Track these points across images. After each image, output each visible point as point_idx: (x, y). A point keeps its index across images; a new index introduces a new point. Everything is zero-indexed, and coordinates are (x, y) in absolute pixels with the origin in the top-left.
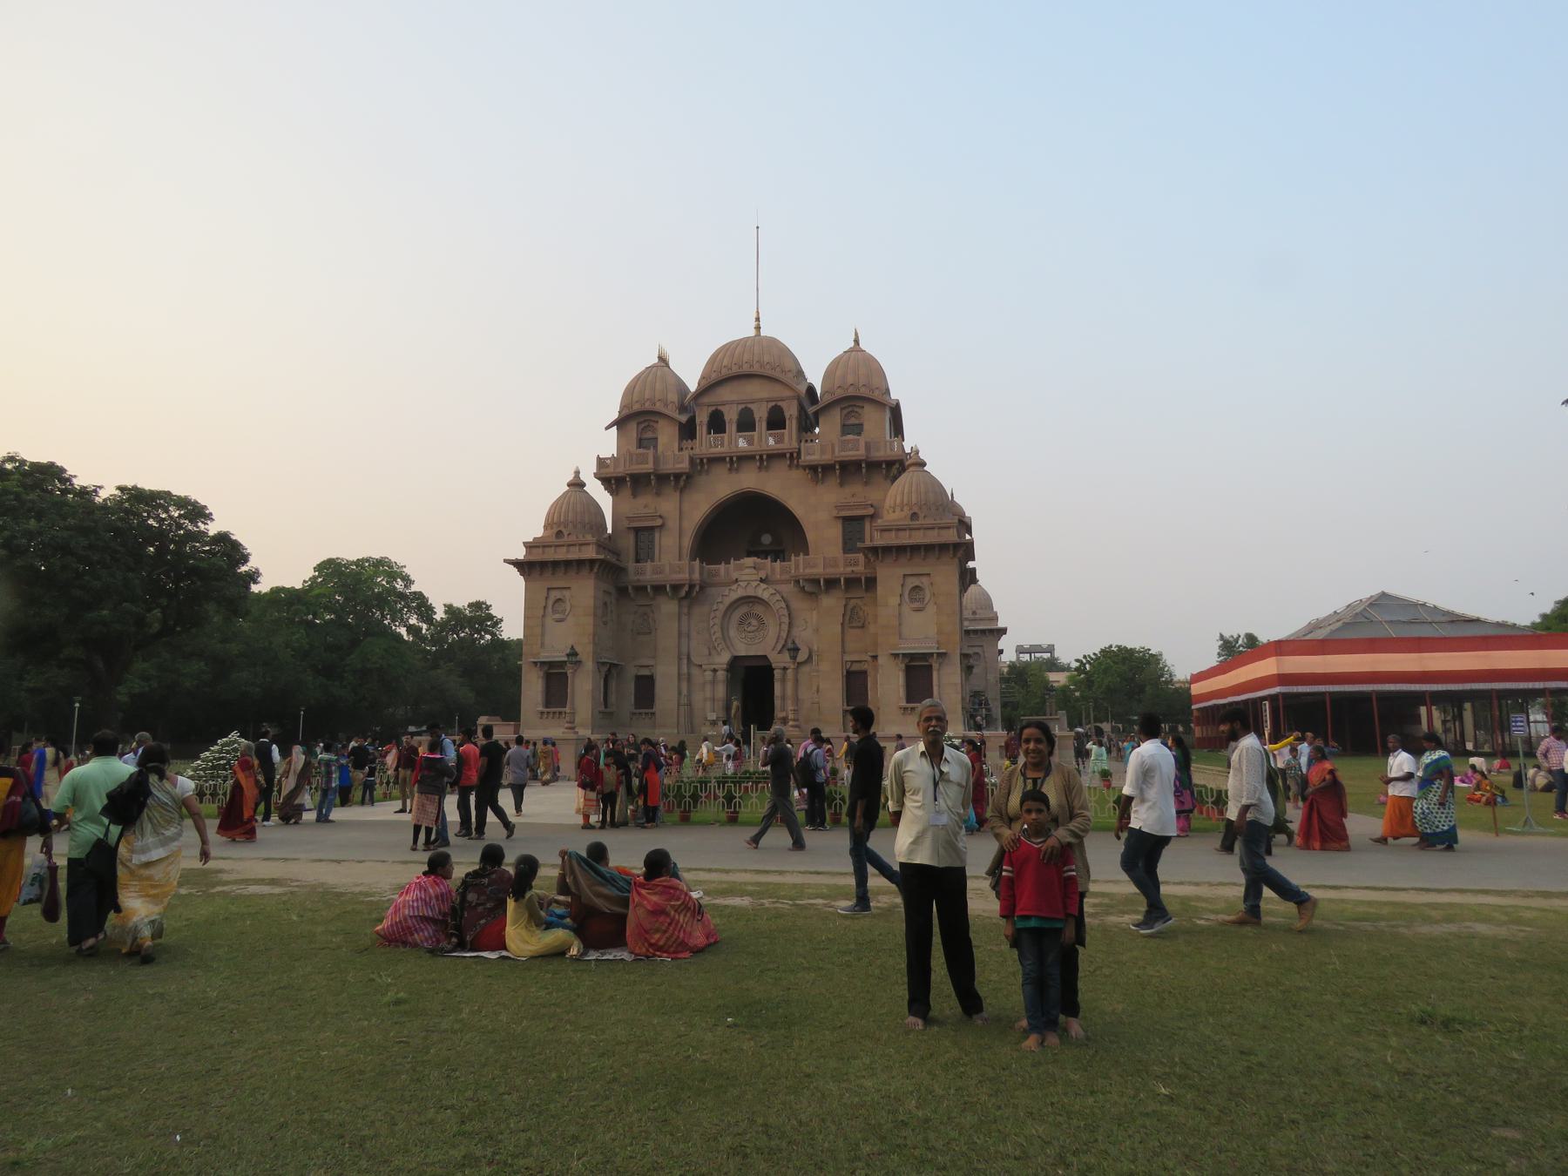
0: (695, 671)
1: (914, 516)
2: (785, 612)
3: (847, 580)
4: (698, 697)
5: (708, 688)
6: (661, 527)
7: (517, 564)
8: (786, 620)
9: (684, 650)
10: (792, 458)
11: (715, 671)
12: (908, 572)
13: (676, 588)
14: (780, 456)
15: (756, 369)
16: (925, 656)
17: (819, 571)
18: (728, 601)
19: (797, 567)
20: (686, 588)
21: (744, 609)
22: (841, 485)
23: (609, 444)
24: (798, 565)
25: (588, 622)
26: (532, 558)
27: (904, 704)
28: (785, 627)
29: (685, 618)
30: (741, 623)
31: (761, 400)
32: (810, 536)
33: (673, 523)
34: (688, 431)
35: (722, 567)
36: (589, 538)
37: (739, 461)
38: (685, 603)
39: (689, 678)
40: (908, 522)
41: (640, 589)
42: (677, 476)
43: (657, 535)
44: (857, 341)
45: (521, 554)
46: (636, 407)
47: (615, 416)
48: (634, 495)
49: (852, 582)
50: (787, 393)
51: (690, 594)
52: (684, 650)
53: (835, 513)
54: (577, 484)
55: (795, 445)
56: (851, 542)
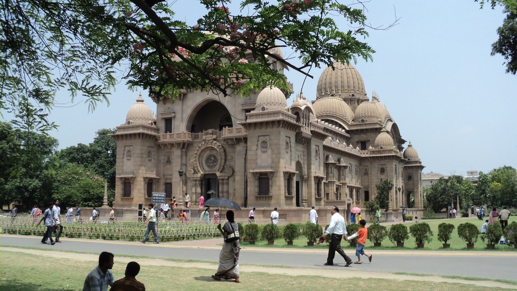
2: (223, 154)
6: (174, 117)
8: (223, 157)
13: (179, 144)
16: (266, 174)
20: (182, 145)
24: (226, 133)
28: (223, 161)
29: (184, 157)
30: (208, 159)
33: (178, 116)
35: (200, 134)
38: (184, 150)
40: (261, 111)
41: (165, 145)
48: (164, 103)
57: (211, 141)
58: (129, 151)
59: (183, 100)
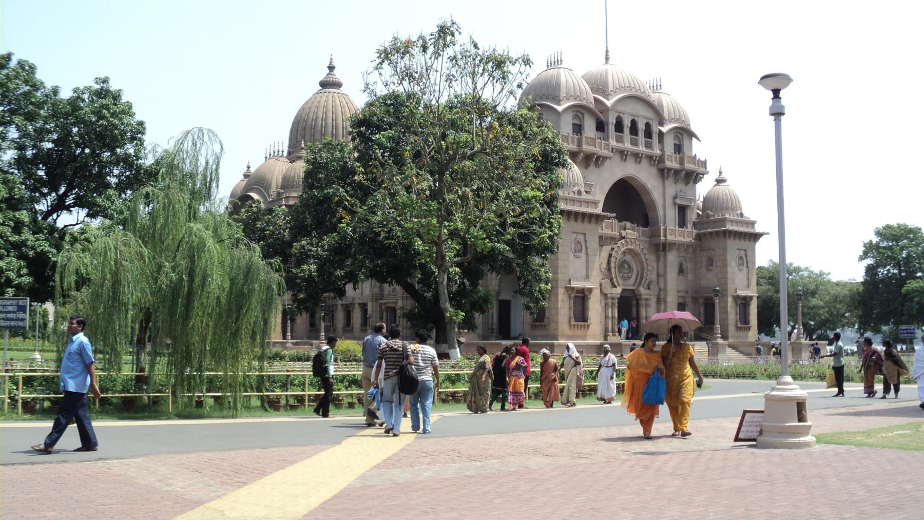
11: (612, 299)
14: (650, 158)
34: (601, 126)
42: (605, 158)
53: (678, 201)
56: (682, 223)
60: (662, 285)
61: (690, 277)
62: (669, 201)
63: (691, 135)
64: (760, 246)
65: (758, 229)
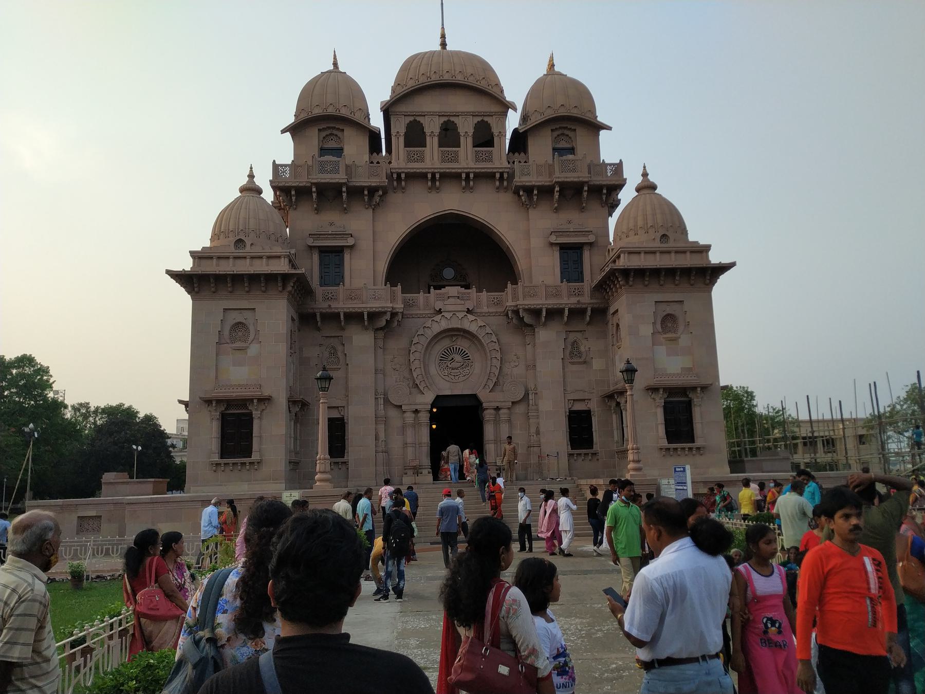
0: (393, 413)
1: (664, 237)
3: (571, 311)
4: (396, 444)
5: (409, 432)
6: (351, 247)
7: (180, 277)
9: (381, 390)
10: (500, 180)
11: (416, 412)
12: (660, 297)
13: (374, 316)
14: (489, 176)
15: (459, 78)
17: (541, 301)
18: (430, 334)
19: (515, 298)
20: (388, 317)
21: (446, 343)
22: (556, 210)
23: (285, 151)
25: (282, 349)
26: (200, 270)
27: (664, 443)
29: (380, 351)
30: (444, 357)
31: (466, 114)
32: (521, 264)
35: (421, 297)
36: (278, 250)
37: (436, 180)
38: (381, 334)
39: (386, 421)
40: (657, 244)
41: (332, 317)
42: (373, 191)
43: (347, 257)
44: (552, 66)
45: (187, 265)
46: (317, 112)
47: (290, 120)
49: (577, 313)
50: (495, 108)
51: (383, 324)
52: (381, 390)
53: (553, 239)
54: (251, 189)
55: (506, 164)
57: (460, 315)
58: (239, 326)
59: (375, 207)
60: (531, 386)
61: (597, 364)
62: (537, 242)
63: (596, 127)
64: (721, 289)
65: (715, 258)
